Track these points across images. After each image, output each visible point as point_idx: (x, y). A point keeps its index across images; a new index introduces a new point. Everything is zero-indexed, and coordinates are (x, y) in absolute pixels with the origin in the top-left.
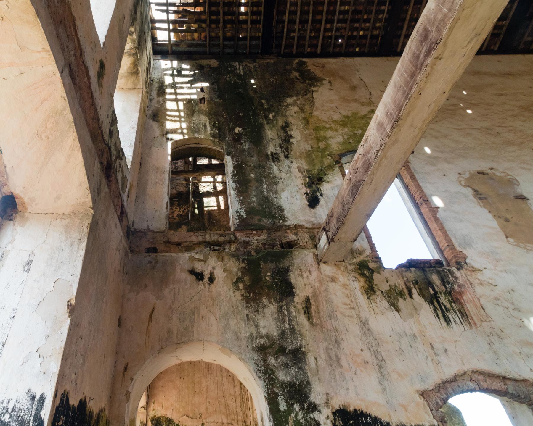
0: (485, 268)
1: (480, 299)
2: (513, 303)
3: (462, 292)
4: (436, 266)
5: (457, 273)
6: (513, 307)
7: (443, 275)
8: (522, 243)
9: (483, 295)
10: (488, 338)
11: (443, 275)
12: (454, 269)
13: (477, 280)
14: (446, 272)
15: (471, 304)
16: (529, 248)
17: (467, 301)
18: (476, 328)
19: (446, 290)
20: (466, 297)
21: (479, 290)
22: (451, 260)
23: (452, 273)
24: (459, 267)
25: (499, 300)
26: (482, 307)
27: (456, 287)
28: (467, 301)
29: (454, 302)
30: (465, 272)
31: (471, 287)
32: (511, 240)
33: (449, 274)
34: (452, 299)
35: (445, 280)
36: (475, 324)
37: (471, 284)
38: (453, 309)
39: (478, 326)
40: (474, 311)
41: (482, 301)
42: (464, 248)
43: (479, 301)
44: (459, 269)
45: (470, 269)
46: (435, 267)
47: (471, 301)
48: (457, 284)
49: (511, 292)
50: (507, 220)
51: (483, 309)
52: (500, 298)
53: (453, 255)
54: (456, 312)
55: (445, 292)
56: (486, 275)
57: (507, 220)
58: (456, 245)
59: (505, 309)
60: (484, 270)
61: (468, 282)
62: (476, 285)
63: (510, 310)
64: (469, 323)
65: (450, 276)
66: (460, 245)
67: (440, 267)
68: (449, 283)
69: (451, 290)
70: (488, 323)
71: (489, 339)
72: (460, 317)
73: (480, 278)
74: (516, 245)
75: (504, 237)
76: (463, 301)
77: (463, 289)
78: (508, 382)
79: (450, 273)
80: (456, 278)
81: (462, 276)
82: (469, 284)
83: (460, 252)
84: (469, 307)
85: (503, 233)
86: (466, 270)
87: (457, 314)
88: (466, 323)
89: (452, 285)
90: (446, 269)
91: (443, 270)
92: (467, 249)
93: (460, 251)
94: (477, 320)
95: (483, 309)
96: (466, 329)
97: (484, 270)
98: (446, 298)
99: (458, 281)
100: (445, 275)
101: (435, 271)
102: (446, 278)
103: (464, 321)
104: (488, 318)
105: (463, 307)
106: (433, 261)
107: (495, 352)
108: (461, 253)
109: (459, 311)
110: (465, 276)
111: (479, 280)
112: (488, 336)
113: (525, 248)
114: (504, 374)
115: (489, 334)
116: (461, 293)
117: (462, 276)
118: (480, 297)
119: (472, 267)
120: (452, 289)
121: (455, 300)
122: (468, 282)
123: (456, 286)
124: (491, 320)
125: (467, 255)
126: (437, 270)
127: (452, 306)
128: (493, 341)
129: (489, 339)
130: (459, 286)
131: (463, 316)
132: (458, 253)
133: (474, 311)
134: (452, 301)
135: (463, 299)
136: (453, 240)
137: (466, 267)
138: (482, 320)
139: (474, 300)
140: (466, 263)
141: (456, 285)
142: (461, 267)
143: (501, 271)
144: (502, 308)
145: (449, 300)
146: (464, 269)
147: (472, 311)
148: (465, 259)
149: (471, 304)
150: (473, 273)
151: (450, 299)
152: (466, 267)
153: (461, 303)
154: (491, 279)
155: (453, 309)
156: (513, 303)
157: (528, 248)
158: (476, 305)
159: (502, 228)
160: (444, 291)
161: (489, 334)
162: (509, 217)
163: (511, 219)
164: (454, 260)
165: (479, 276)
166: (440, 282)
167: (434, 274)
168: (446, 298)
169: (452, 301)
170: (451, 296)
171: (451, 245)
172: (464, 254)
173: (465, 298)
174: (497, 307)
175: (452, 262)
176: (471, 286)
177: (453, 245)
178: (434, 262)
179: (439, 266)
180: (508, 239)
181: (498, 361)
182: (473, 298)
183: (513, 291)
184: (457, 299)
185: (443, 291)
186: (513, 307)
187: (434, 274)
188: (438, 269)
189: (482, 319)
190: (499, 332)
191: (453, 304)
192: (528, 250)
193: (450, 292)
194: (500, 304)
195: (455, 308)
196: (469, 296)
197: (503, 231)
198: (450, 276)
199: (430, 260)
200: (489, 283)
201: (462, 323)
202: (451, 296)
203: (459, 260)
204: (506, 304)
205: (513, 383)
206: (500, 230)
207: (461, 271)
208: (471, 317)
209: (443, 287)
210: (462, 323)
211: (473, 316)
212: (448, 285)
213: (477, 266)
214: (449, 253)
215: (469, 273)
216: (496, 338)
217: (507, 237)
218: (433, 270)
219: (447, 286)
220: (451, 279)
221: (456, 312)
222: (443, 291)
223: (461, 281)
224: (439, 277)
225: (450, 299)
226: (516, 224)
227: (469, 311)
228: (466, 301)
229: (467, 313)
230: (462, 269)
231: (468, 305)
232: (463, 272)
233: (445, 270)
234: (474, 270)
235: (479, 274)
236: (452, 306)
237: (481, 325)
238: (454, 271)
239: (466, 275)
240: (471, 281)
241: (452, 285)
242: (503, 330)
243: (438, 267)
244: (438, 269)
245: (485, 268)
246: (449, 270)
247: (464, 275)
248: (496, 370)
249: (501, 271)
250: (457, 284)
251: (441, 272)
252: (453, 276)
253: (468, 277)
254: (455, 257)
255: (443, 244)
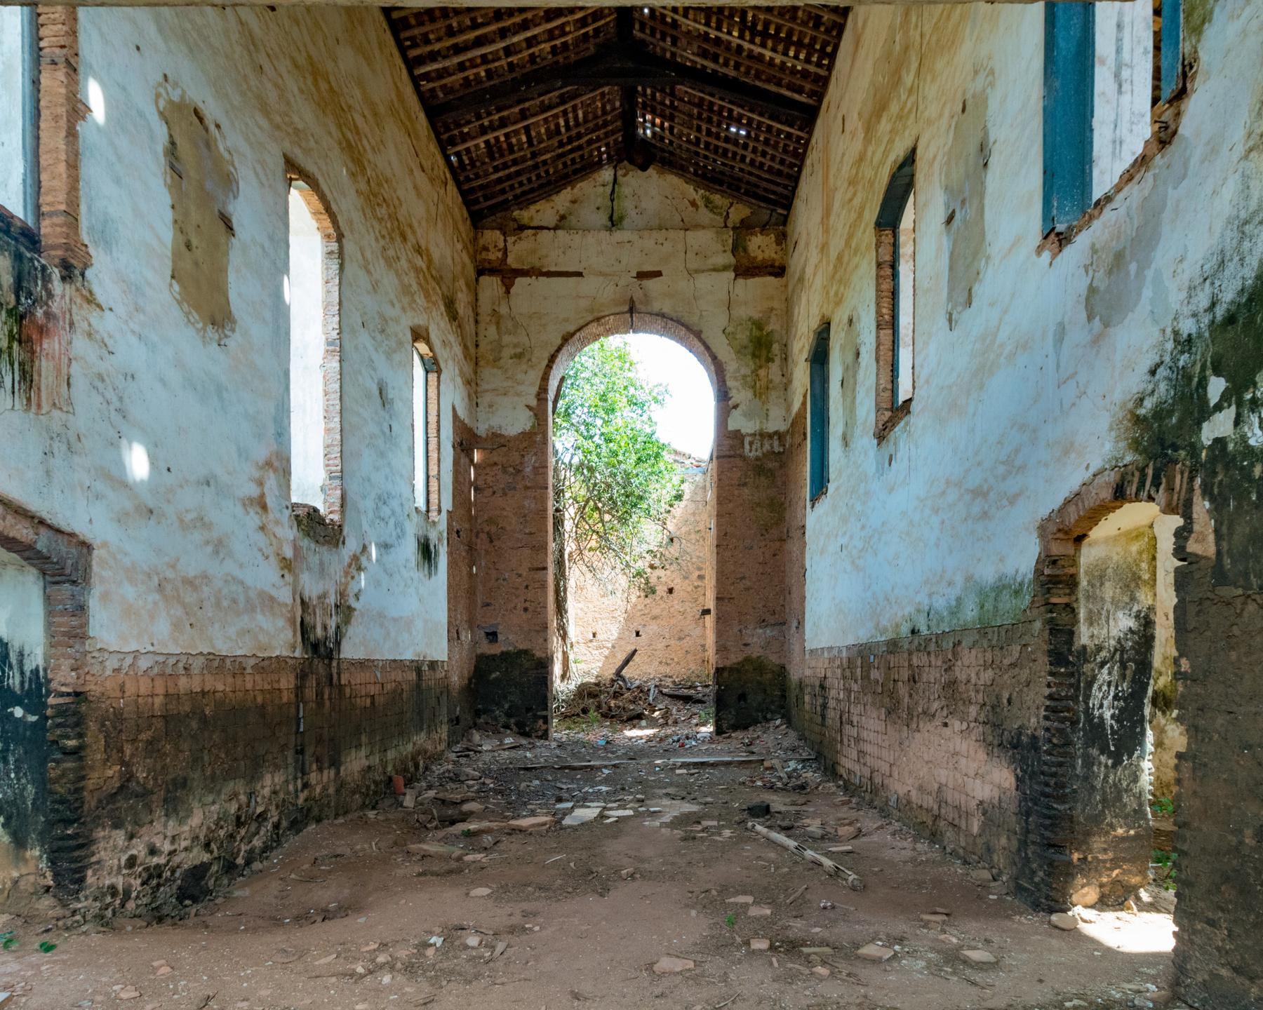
0: (111, 309)
1: (73, 362)
2: (121, 399)
3: (48, 330)
4: (22, 239)
5: (57, 286)
6: (118, 405)
7: (26, 269)
8: (188, 303)
9: (82, 358)
10: (49, 441)
11: (26, 269)
12: (56, 274)
13: (86, 324)
14: (36, 269)
15: (51, 364)
16: (192, 320)
17: (47, 354)
18: (37, 414)
19: (16, 307)
20: (50, 345)
21: (80, 345)
22: (54, 247)
23: (47, 279)
24: (66, 273)
25: (103, 380)
26: (68, 379)
27: (39, 313)
28: (47, 354)
29: (20, 342)
30: (74, 293)
31: (68, 329)
32: (176, 287)
33: (39, 275)
34: (20, 332)
35: (25, 284)
36: (39, 406)
37: (72, 324)
38: (10, 355)
39: (44, 411)
40: (50, 379)
41: (75, 369)
42: (95, 242)
43: (69, 366)
44: (63, 279)
45: (84, 292)
46: (16, 240)
47: (53, 358)
48: (45, 308)
49: (129, 378)
50: (188, 246)
51: (69, 384)
52: (106, 378)
53: (64, 241)
54: (12, 365)
55: (12, 310)
56: (106, 324)
57: (188, 246)
58: (84, 223)
59: (105, 404)
60: (107, 312)
61: (68, 316)
62: (79, 331)
63: (112, 408)
64: (29, 399)
65: (39, 282)
66: (91, 229)
67: (27, 248)
68: (29, 295)
69: (26, 313)
70: (64, 416)
71: (50, 445)
72: (17, 378)
73: (93, 321)
74: (177, 301)
75: (169, 273)
76: (38, 349)
77: (50, 325)
78: (43, 530)
79: (43, 275)
80: (50, 295)
81: (63, 296)
82: (67, 322)
83: (83, 245)
84: (46, 370)
85: (169, 263)
86: (77, 290)
87: (13, 369)
88: (23, 395)
89: (34, 303)
90: (39, 261)
91: (31, 260)
92: (100, 249)
93: (86, 242)
94: (47, 399)
95: (69, 384)
96: (16, 408)
97: (107, 312)
98: (6, 323)
99: (50, 303)
100: (29, 273)
101: (13, 249)
102: (29, 281)
103: (19, 389)
104: (65, 405)
105: (32, 361)
106: (19, 224)
107: (47, 472)
108: (83, 248)
109: (20, 364)
110: (68, 301)
111: (90, 325)
112: (52, 438)
113: (187, 314)
114: (44, 515)
115: (55, 436)
116: (43, 331)
117: (63, 296)
118: (75, 359)
119: (91, 292)
120: (29, 313)
121: (24, 337)
122: (68, 316)
123: (41, 311)
124: (71, 411)
125: (94, 261)
126: (18, 249)
127: (10, 347)
128: (56, 451)
129: (50, 445)
130: (48, 315)
131: (25, 379)
132: (79, 245)
133: (50, 379)
134: (17, 336)
135: (41, 346)
136: (83, 209)
137: (79, 284)
138: (54, 404)
139: (60, 358)
140: (83, 275)
141: (41, 308)
142: (70, 278)
143: (133, 332)
144: (101, 399)
145: (11, 331)
146: (73, 287)
147: (47, 378)
148: (86, 266)
149: (51, 364)
150: (85, 305)
151: (15, 331)
152: (79, 284)
153: (33, 352)
154: (110, 337)
155: (10, 355)
156: (121, 399)
157: (191, 318)
158: (59, 371)
159: (174, 254)
160: (11, 306)
161: (55, 436)
162: (195, 242)
163: (194, 249)
164: (59, 253)
165: (94, 316)
166: (12, 280)
167: (6, 254)
168: (6, 323)
169: (17, 336)
170: (21, 326)
171: (72, 216)
172: (88, 253)
173: (45, 346)
174: (94, 392)
175: (53, 253)
176: (70, 328)
177: (77, 220)
178: (21, 228)
179: (27, 244)
180: (173, 281)
181: (45, 490)
182: (60, 354)
183: (133, 377)
184: (29, 340)
185: (8, 304)
186: (118, 405)
187: (6, 254)
188: (22, 249)
189: (57, 401)
190: (73, 439)
191: (15, 345)
192: (189, 321)
193: (22, 317)
194: (101, 391)
195: (15, 354)
196: (57, 346)
197: (174, 261)
198: (39, 282)
199: (13, 217)
200: (103, 342)
201: (13, 393)
202: (21, 326)
203: (73, 261)
204: (110, 395)
205: (51, 533)
206: (169, 254)
207: (67, 286)
208: (39, 389)
209: (13, 296)
210: (13, 393)
211: (43, 388)
212: (26, 298)
213: (100, 296)
214: (58, 229)
215: (78, 300)
216: (64, 448)
217: (173, 277)
218: (8, 244)
219: (23, 299)
220: (39, 289)
221: (12, 365)
222: (8, 304)
223: (55, 307)
224: (13, 268)
225: (15, 331)
226: (196, 264)
227: (40, 375)
228: (44, 353)
229: (35, 377)
230: (71, 284)
231: (44, 363)
232: (69, 290)
233: (36, 263)
234: (90, 300)
235: (95, 314)
236: (10, 347)
237: (48, 413)
238: (54, 277)
239: (71, 300)
240: (75, 318)
241: (34, 303)
242: (81, 437)
243: (23, 245)
244: (22, 249)
245: (111, 309)
246: (44, 268)
247: (67, 298)
248: (35, 504)
249: (133, 332)
250: (45, 308)
251: (25, 261)
252: (45, 287)
253: (74, 307)
254: (67, 247)
255: (54, 199)
